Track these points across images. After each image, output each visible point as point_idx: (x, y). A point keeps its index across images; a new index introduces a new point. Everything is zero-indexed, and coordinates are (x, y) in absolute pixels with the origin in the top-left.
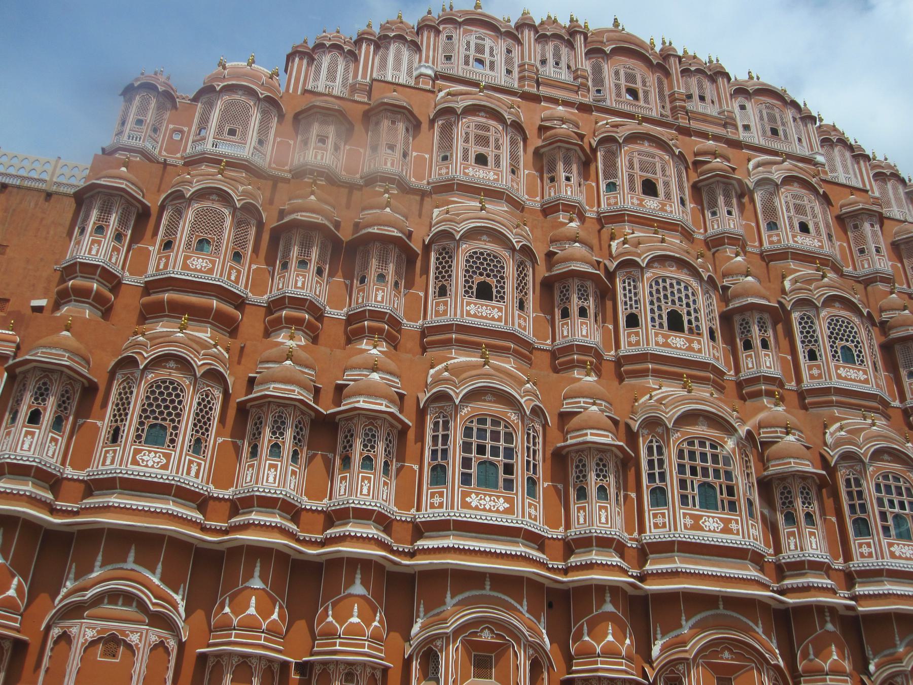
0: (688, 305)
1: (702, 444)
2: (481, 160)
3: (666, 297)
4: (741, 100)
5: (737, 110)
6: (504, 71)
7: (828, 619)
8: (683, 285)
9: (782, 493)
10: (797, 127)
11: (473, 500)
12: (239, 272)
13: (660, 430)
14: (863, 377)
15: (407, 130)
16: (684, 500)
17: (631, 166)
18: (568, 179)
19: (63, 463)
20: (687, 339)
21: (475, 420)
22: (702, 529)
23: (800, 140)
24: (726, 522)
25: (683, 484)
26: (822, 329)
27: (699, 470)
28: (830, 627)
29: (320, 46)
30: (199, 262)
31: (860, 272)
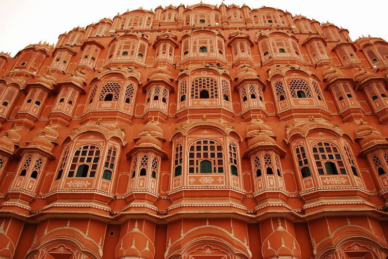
0: (212, 87)
2: (125, 53)
3: (200, 85)
4: (255, 14)
5: (253, 18)
7: (280, 224)
8: (210, 79)
9: (255, 161)
12: (5, 109)
13: (181, 138)
15: (96, 50)
16: (191, 170)
17: (195, 43)
18: (164, 53)
20: (210, 101)
21: (82, 147)
22: (201, 183)
23: (283, 23)
25: (192, 162)
27: (202, 155)
28: (280, 228)
29: (71, 32)
31: (314, 63)
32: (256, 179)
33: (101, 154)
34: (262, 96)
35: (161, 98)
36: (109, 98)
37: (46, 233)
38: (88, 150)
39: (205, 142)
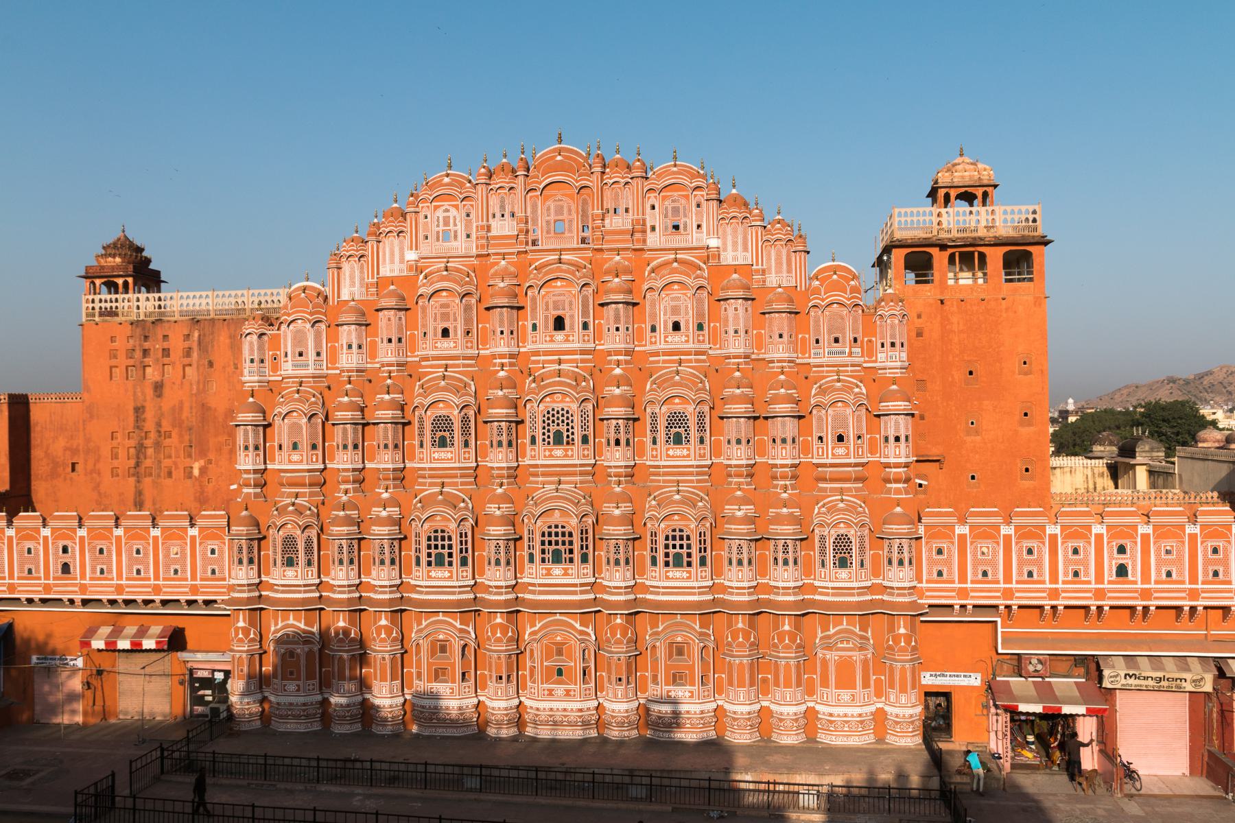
1: (556, 527)
2: (445, 333)
4: (652, 199)
6: (464, 236)
10: (699, 215)
11: (433, 574)
14: (685, 452)
15: (400, 319)
16: (543, 560)
17: (547, 309)
18: (502, 333)
19: (259, 576)
23: (699, 226)
24: (566, 570)
25: (543, 552)
26: (662, 424)
30: (295, 457)
32: (605, 567)
33: (454, 542)
34: (630, 436)
35: (505, 443)
36: (443, 443)
37: (424, 623)
38: (440, 534)
39: (556, 527)
